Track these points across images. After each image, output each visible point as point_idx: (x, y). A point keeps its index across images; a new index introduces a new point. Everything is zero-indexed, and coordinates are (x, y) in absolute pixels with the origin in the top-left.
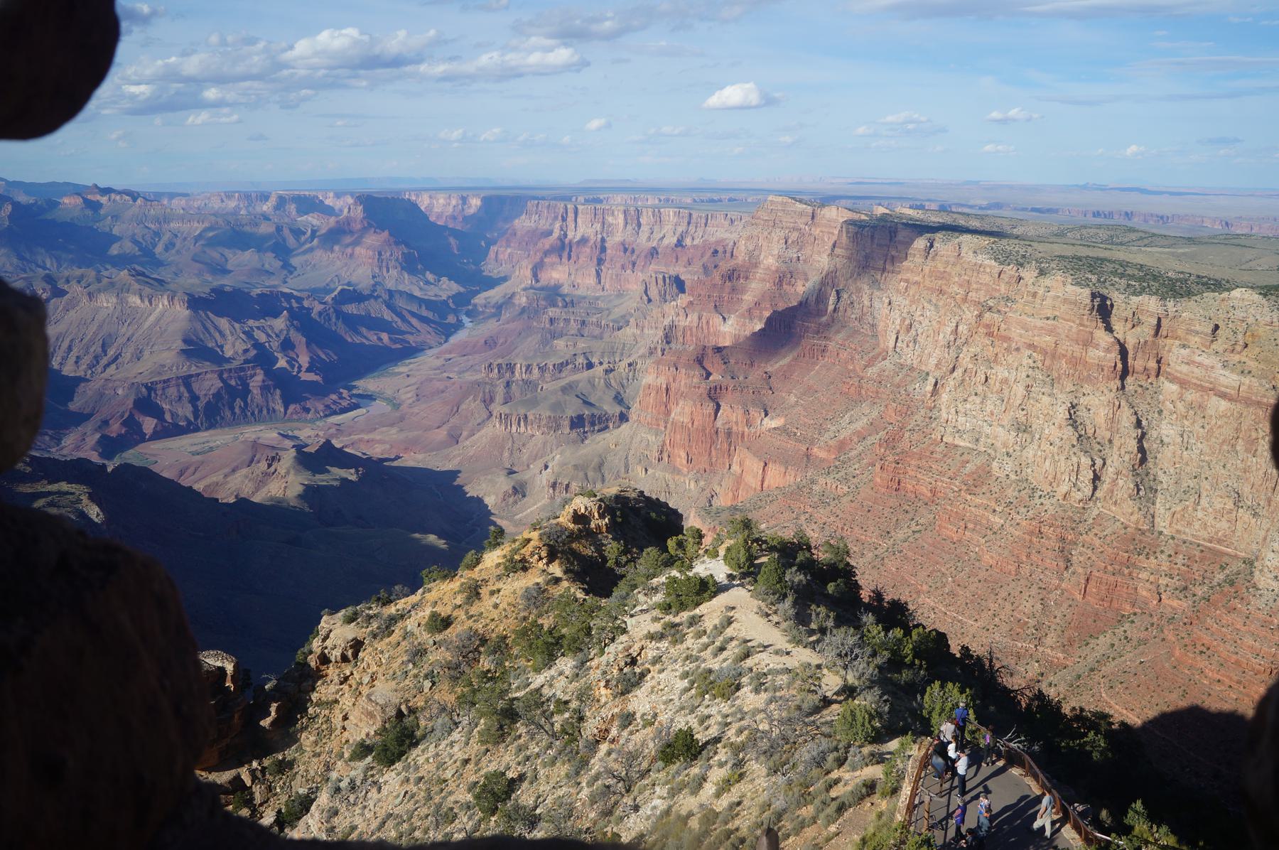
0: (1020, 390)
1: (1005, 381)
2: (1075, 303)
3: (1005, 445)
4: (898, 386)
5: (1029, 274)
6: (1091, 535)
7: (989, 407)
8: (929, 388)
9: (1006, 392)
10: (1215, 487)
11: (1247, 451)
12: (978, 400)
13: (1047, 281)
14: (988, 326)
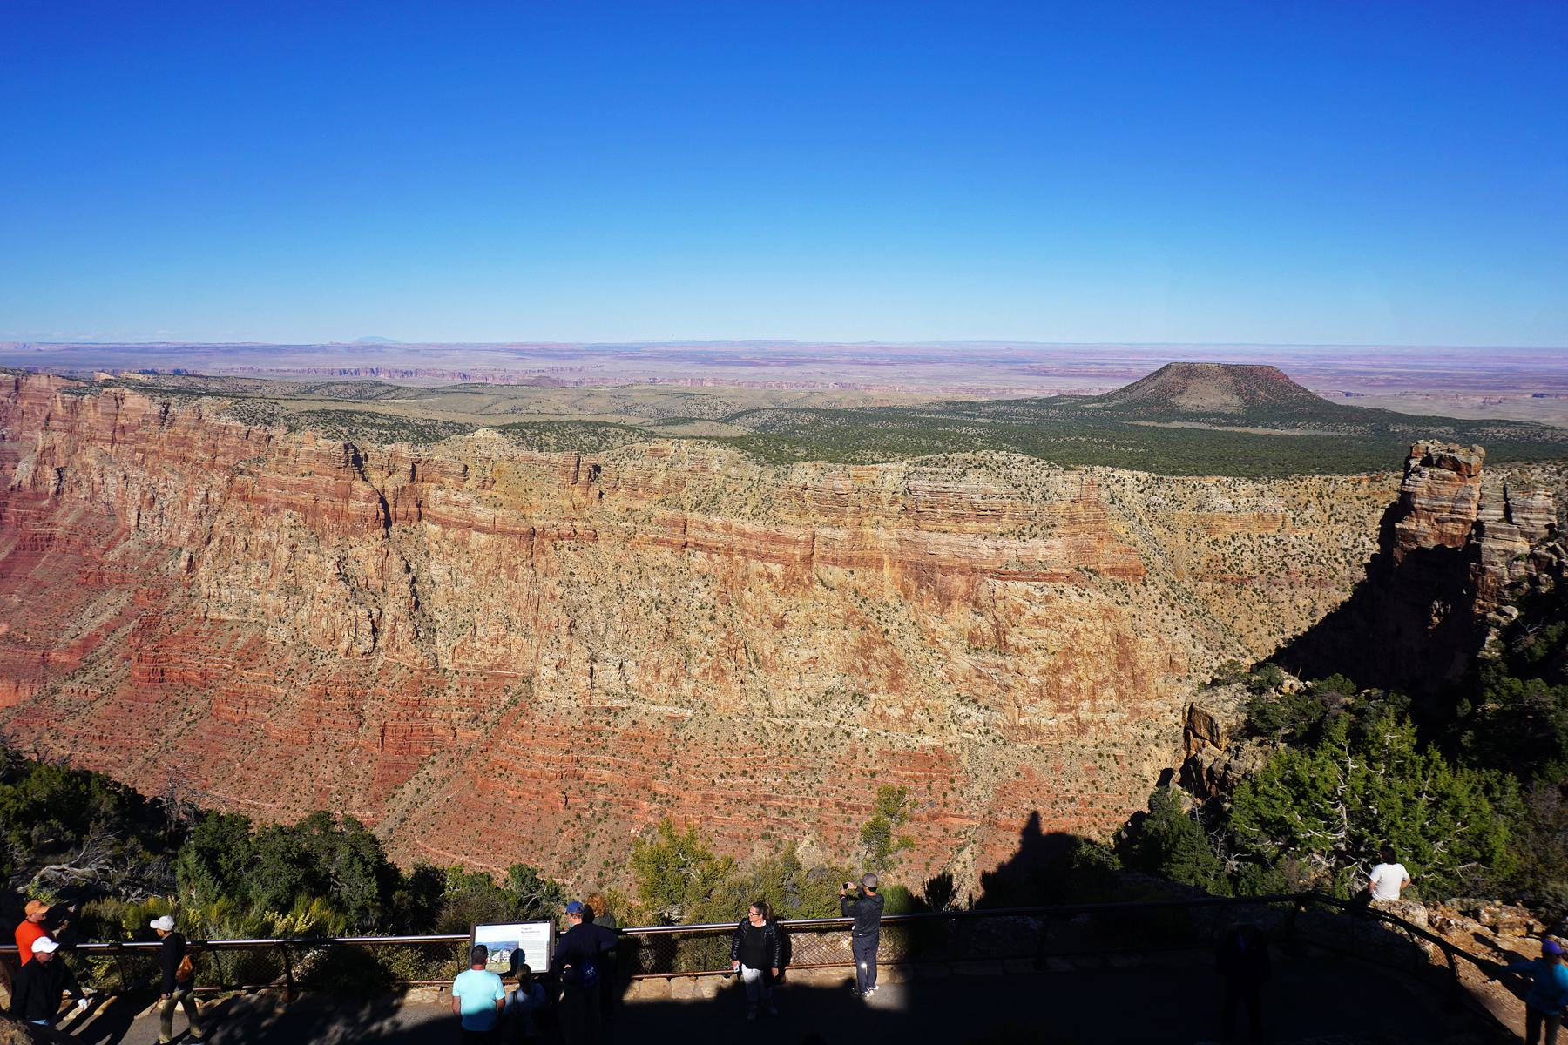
0: (285, 552)
1: (267, 545)
2: (329, 456)
3: (277, 611)
4: (148, 567)
5: (279, 433)
6: (379, 685)
7: (254, 574)
8: (184, 564)
9: (270, 556)
10: (487, 616)
11: (510, 578)
12: (241, 568)
13: (298, 437)
14: (241, 490)
